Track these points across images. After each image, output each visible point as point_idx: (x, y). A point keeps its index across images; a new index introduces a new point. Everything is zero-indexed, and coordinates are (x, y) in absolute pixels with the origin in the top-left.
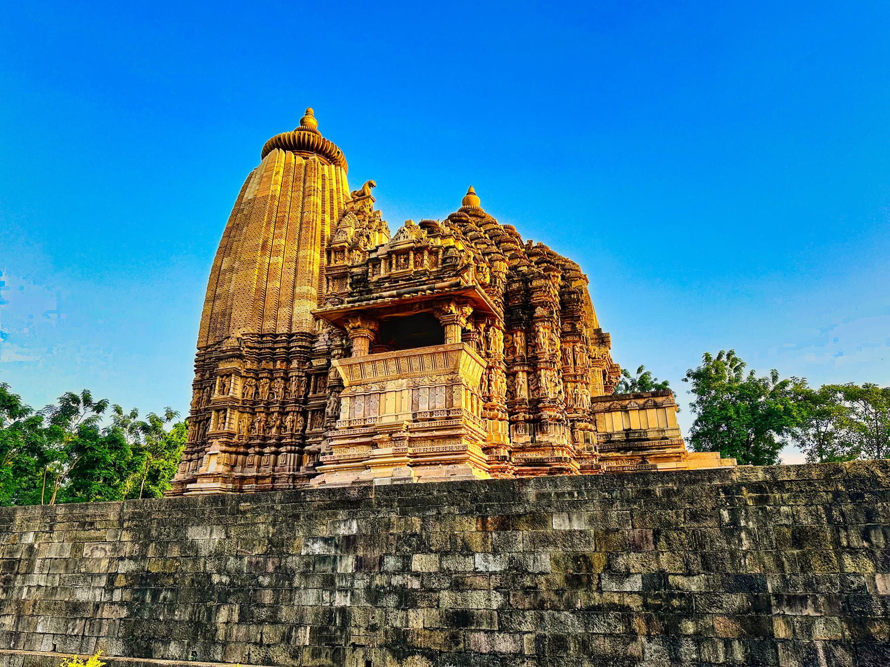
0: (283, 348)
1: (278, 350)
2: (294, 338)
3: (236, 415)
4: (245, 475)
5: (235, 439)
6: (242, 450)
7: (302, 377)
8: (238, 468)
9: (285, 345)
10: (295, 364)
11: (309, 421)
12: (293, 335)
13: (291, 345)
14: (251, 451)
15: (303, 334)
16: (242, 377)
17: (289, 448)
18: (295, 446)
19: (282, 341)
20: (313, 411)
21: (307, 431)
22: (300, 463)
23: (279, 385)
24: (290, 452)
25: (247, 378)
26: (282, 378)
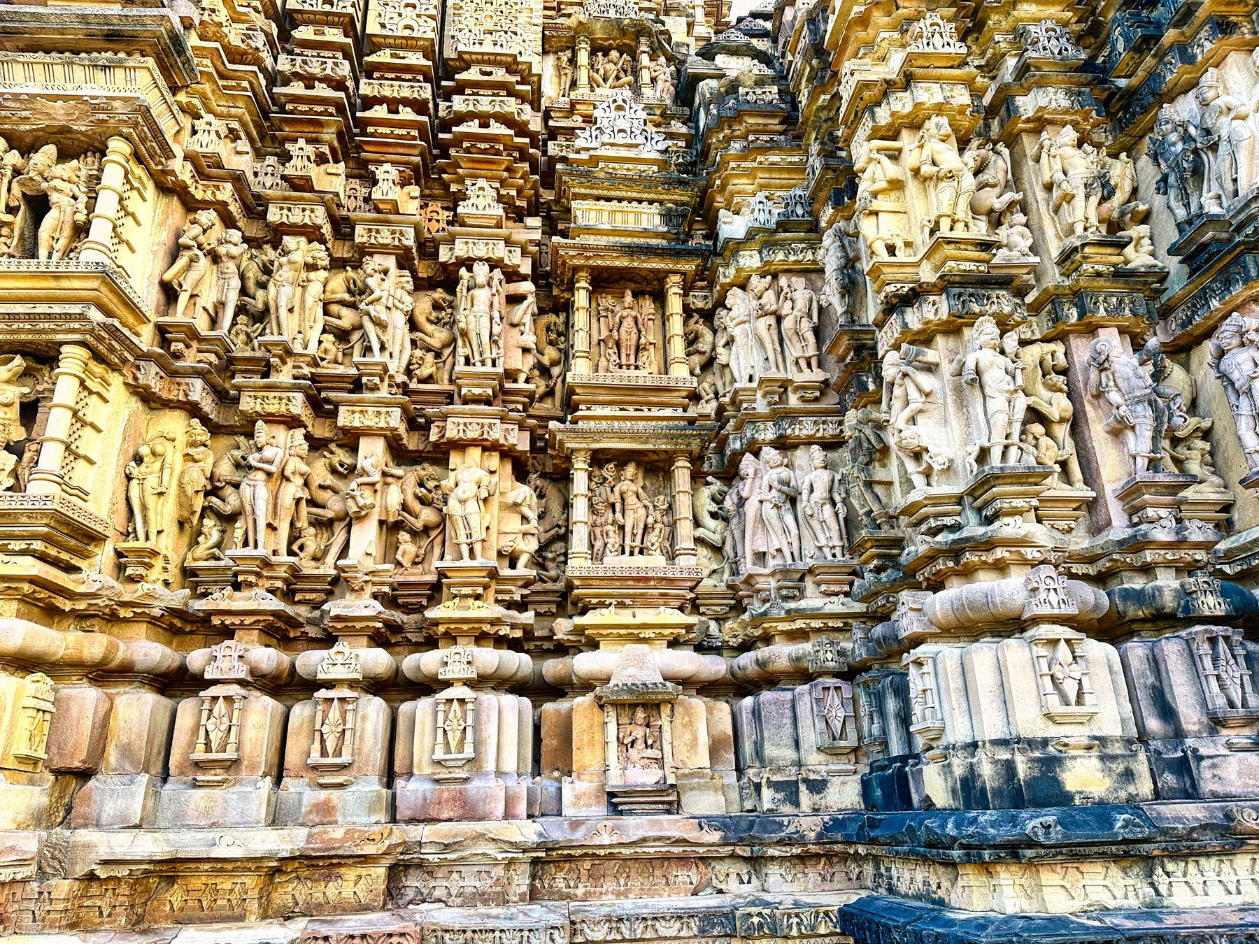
0: (406, 102)
1: (380, 112)
2: (473, 74)
3: (115, 407)
4: (189, 843)
5: (95, 575)
6: (148, 650)
7: (512, 275)
8: (119, 794)
9: (427, 92)
10: (481, 200)
11: (580, 510)
12: (465, 62)
13: (459, 104)
14: (219, 661)
15: (512, 66)
16: (167, 187)
17: (490, 658)
18: (501, 642)
19: (401, 71)
20: (598, 459)
21: (578, 565)
22: (549, 753)
23: (390, 288)
24: (480, 682)
25: (205, 205)
26: (404, 261)
